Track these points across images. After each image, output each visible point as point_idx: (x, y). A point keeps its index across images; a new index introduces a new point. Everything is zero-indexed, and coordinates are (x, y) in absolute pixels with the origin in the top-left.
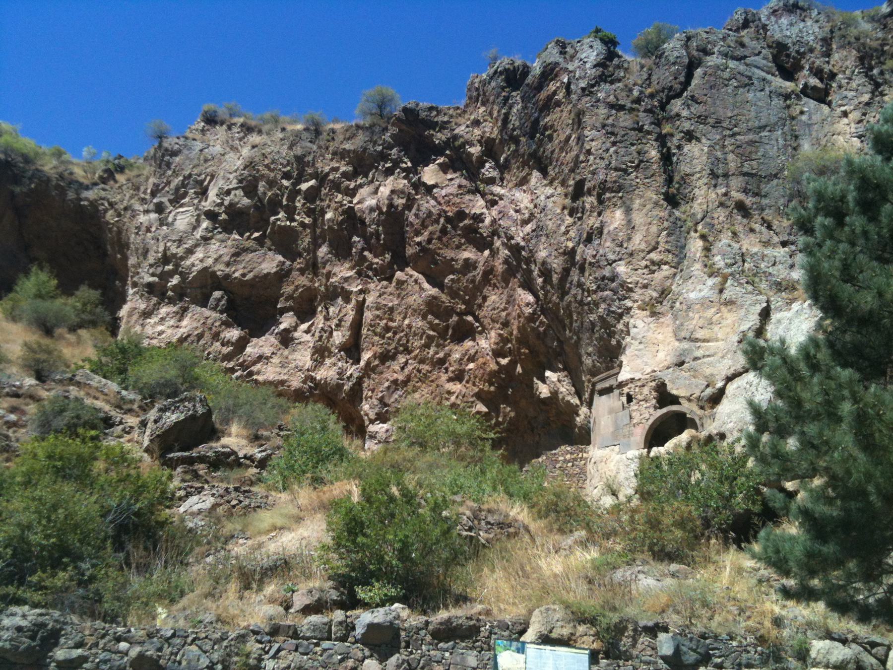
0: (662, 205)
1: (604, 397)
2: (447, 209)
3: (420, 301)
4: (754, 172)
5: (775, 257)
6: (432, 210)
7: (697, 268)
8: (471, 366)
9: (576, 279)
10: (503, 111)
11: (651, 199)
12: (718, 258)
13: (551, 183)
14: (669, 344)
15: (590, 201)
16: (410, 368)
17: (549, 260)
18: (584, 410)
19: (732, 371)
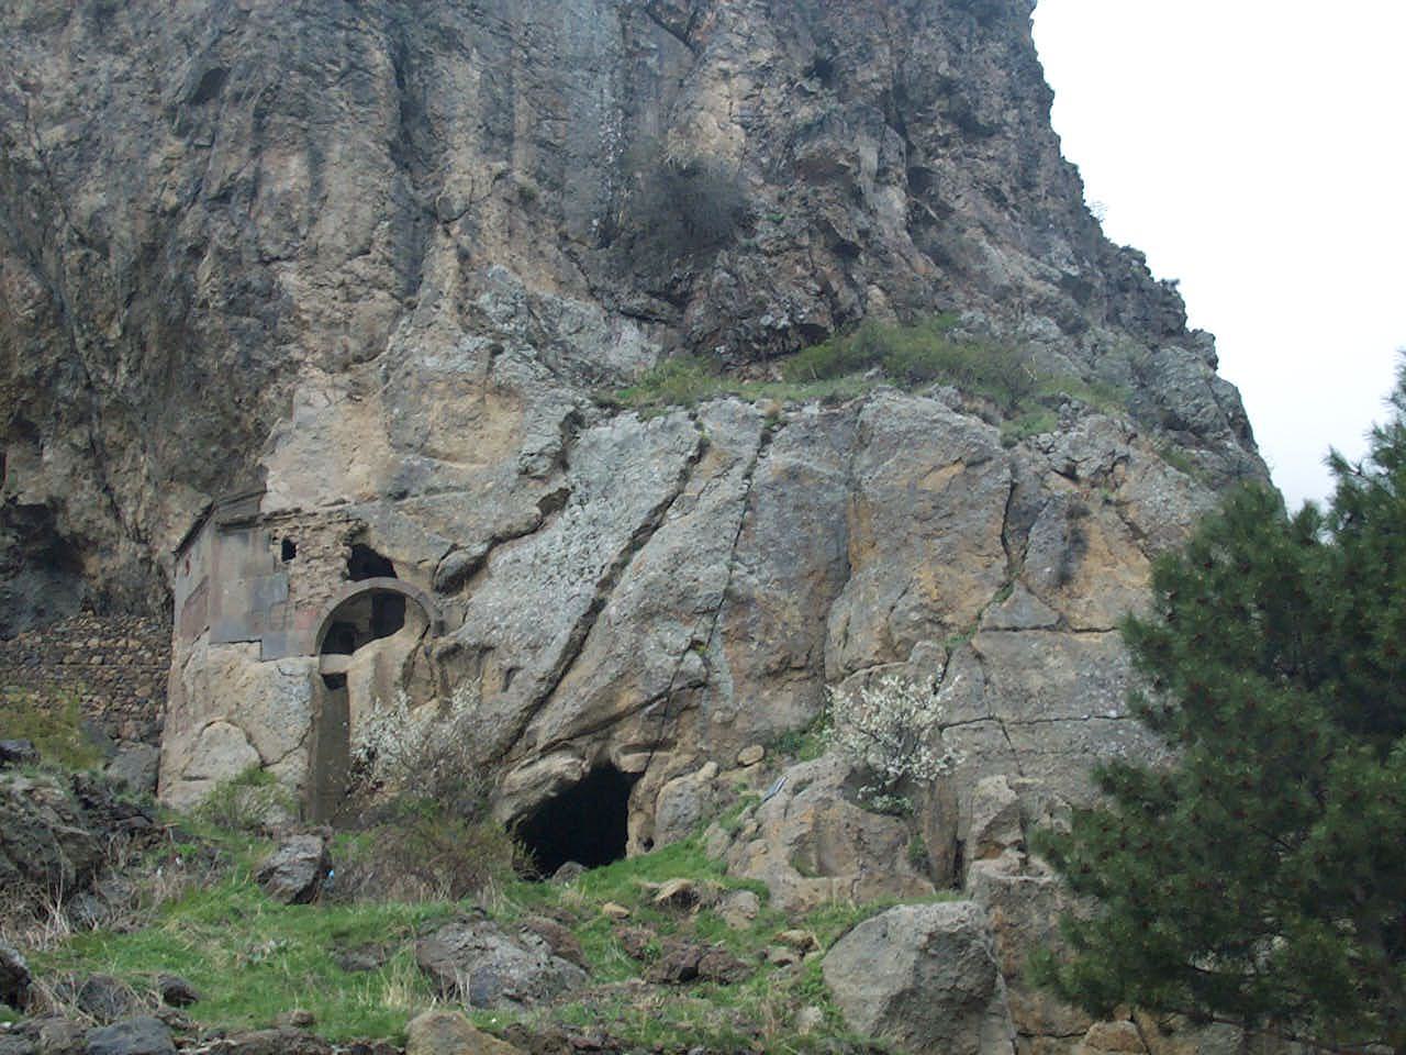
0: (386, 167)
1: (233, 544)
5: (582, 315)
9: (173, 273)
13: (121, 50)
17: (109, 219)
18: (126, 550)
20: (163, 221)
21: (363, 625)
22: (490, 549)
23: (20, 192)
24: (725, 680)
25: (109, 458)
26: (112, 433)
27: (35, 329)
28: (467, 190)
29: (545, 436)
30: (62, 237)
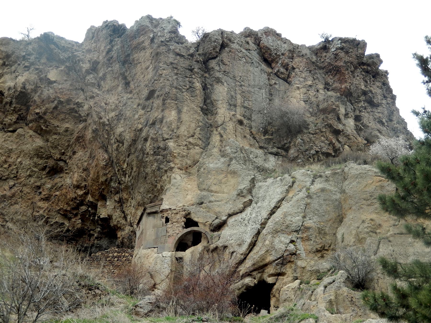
1: (151, 218)
2: (60, 97)
3: (31, 148)
4: (249, 107)
5: (257, 153)
6: (51, 95)
7: (215, 151)
8: (57, 193)
9: (140, 147)
10: (108, 47)
11: (193, 108)
12: (228, 148)
13: (131, 92)
14: (194, 191)
15: (157, 102)
16: (15, 189)
17: (124, 134)
18: (128, 229)
19: (232, 211)
20: (138, 133)
21: (190, 243)
22: (228, 218)
23: (103, 131)
24: (302, 252)
25: (124, 203)
26: (125, 195)
27: (106, 168)
28: (223, 119)
29: (245, 185)
30: (112, 141)
